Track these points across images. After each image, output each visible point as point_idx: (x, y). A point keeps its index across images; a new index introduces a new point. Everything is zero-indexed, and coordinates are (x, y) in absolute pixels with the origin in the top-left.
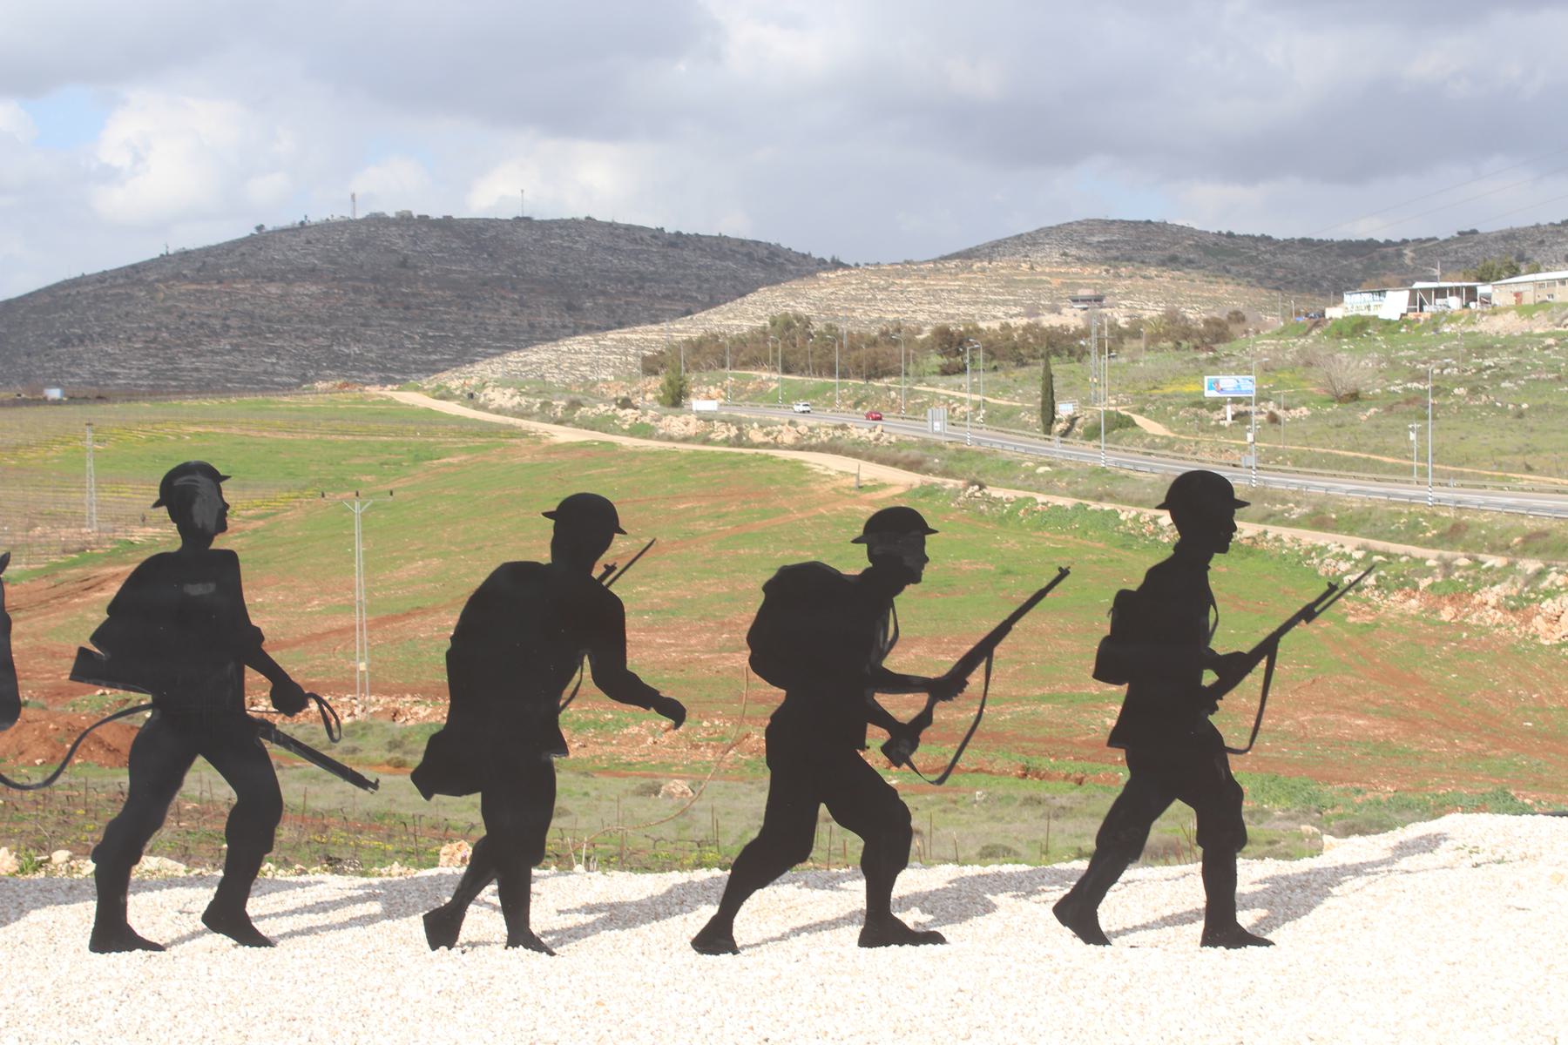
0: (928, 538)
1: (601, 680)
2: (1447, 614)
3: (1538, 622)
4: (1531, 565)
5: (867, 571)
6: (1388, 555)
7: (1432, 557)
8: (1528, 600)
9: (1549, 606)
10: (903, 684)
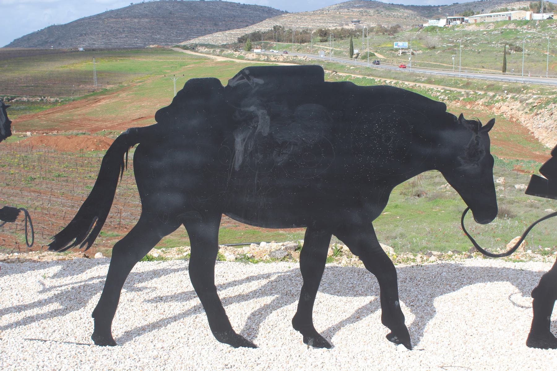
2: (468, 107)
3: (494, 109)
4: (491, 94)
6: (451, 91)
7: (463, 91)
8: (491, 103)
9: (497, 105)
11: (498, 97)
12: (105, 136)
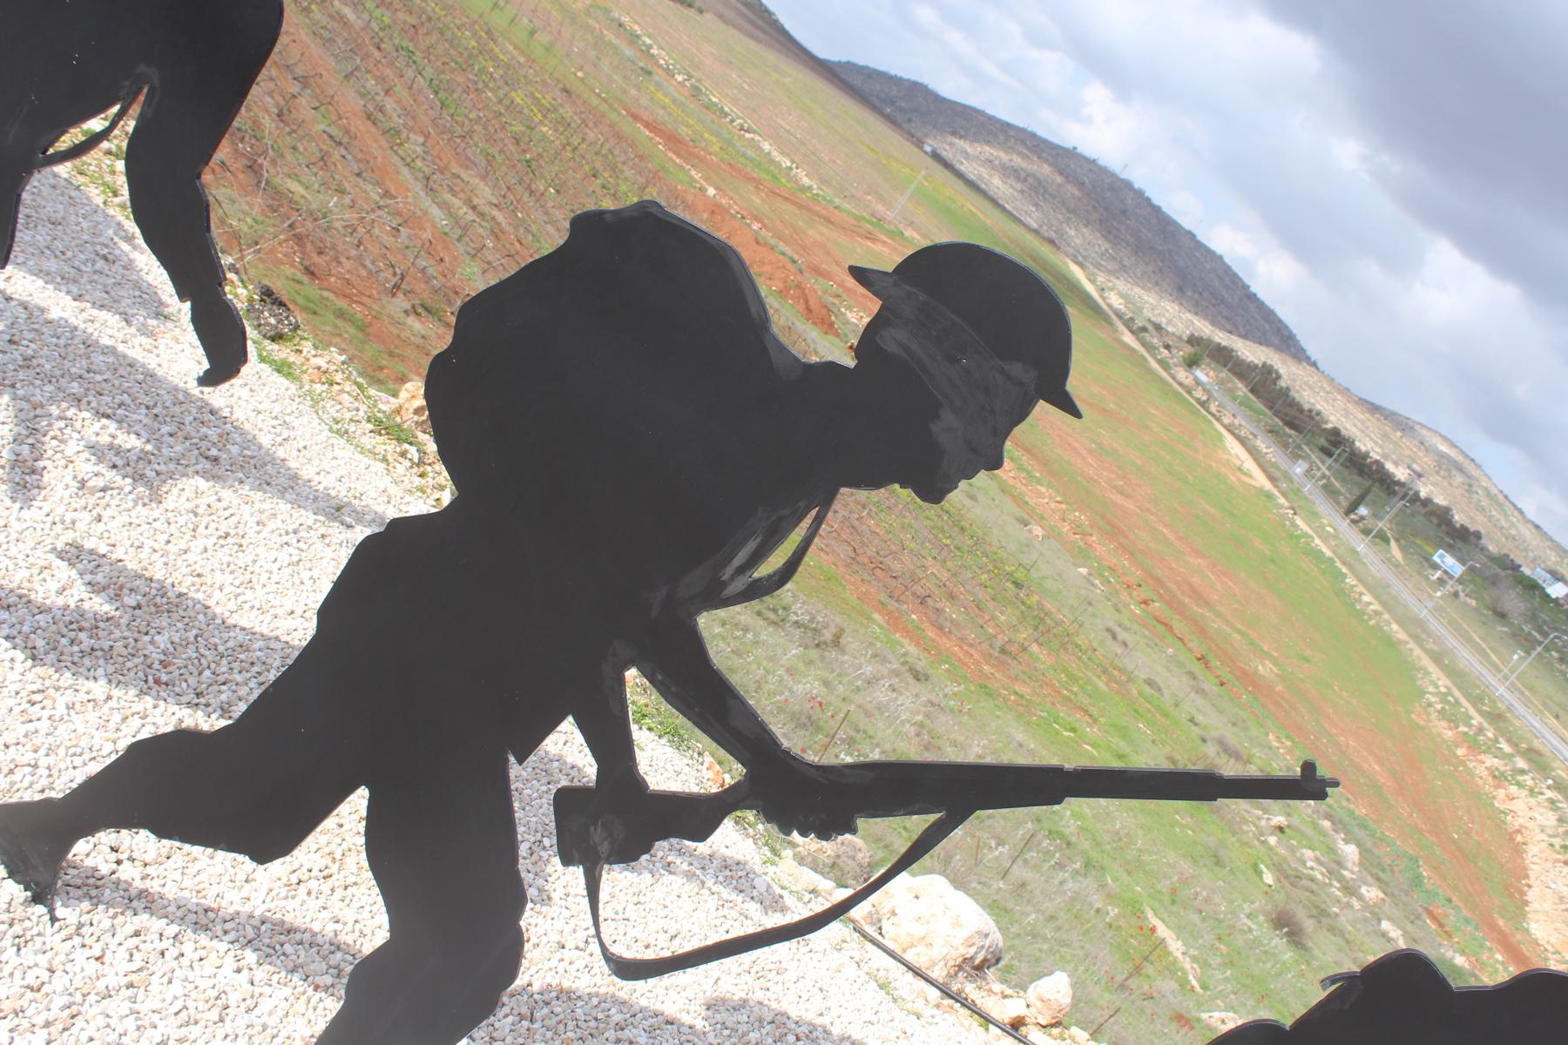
0: (1043, 409)
1: (134, 157)
2: (1460, 752)
3: (1501, 793)
4: (1521, 763)
5: (831, 369)
6: (1457, 701)
7: (1477, 720)
9: (1513, 789)
10: (711, 704)
11: (1527, 780)
12: (825, 292)
